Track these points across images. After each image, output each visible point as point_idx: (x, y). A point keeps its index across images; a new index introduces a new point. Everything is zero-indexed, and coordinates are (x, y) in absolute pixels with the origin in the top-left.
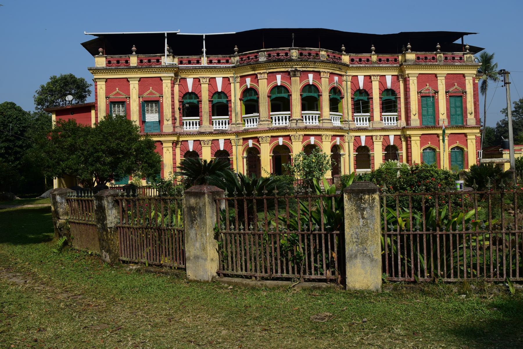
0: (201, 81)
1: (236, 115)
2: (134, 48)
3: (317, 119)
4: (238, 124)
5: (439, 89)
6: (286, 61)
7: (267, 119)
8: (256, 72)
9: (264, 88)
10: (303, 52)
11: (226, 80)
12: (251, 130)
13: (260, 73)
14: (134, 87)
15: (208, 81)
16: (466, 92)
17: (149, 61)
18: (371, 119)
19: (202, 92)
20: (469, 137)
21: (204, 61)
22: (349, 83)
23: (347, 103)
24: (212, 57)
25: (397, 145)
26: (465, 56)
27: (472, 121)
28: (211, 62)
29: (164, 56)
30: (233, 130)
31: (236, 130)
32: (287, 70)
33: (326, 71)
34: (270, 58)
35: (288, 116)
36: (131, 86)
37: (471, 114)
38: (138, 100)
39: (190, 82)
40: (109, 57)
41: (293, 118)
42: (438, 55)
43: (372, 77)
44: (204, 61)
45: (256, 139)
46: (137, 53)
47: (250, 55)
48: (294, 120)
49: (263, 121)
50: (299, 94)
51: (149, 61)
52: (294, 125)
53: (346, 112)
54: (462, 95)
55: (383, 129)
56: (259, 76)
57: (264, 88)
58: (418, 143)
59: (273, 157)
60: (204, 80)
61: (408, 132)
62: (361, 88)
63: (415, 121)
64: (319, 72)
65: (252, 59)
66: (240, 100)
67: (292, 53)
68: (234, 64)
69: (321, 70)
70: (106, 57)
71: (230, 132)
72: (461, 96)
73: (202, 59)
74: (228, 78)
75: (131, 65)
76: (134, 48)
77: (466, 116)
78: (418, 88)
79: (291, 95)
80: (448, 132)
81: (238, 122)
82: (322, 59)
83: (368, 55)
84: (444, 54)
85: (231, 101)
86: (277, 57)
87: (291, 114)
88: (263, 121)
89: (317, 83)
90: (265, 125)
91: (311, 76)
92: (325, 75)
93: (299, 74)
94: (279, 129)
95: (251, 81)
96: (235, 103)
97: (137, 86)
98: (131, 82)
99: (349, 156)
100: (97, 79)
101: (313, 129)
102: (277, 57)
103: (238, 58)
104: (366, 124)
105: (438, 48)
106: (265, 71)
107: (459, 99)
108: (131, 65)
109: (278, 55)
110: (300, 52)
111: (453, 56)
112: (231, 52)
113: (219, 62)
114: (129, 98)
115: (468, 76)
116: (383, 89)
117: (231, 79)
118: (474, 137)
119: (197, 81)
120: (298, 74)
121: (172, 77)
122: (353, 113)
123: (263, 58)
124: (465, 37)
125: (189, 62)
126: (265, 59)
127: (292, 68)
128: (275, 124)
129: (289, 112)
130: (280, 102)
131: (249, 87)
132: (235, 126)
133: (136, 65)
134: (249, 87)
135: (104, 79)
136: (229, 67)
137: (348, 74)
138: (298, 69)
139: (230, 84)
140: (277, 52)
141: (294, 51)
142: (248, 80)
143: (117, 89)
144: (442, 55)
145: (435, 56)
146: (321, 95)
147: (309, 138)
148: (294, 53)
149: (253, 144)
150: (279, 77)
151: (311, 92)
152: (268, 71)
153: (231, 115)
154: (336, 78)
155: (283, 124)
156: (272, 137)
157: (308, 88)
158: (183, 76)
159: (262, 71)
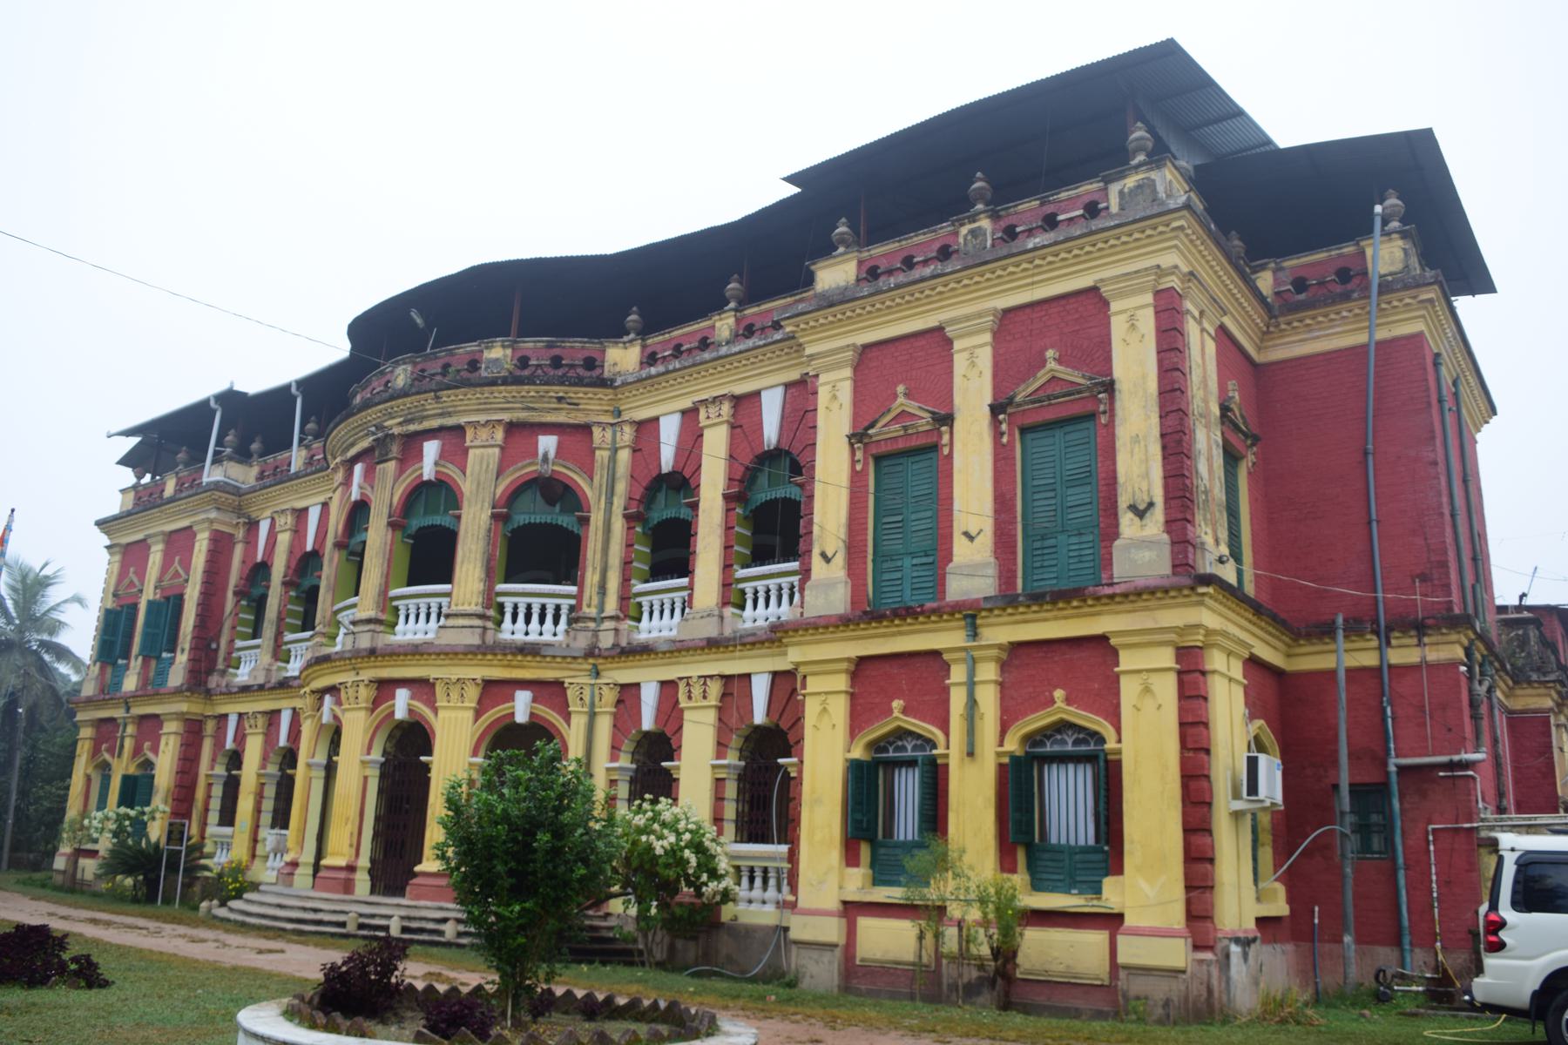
5: (957, 400)
16: (1110, 387)
20: (1127, 661)
22: (624, 456)
23: (608, 539)
25: (784, 725)
26: (1114, 189)
27: (1147, 555)
33: (482, 418)
37: (1140, 513)
53: (597, 578)
54: (1090, 407)
55: (714, 645)
58: (839, 708)
63: (829, 584)
64: (460, 430)
69: (462, 420)
72: (1085, 413)
80: (1002, 632)
82: (484, 374)
84: (995, 217)
89: (452, 471)
91: (431, 449)
92: (484, 434)
105: (980, 196)
107: (1076, 434)
111: (1049, 209)
115: (1122, 294)
118: (1166, 657)
120: (395, 449)
121: (211, 521)
122: (625, 581)
137: (626, 416)
138: (396, 431)
144: (985, 223)
145: (949, 241)
147: (393, 697)
151: (436, 511)
154: (547, 443)
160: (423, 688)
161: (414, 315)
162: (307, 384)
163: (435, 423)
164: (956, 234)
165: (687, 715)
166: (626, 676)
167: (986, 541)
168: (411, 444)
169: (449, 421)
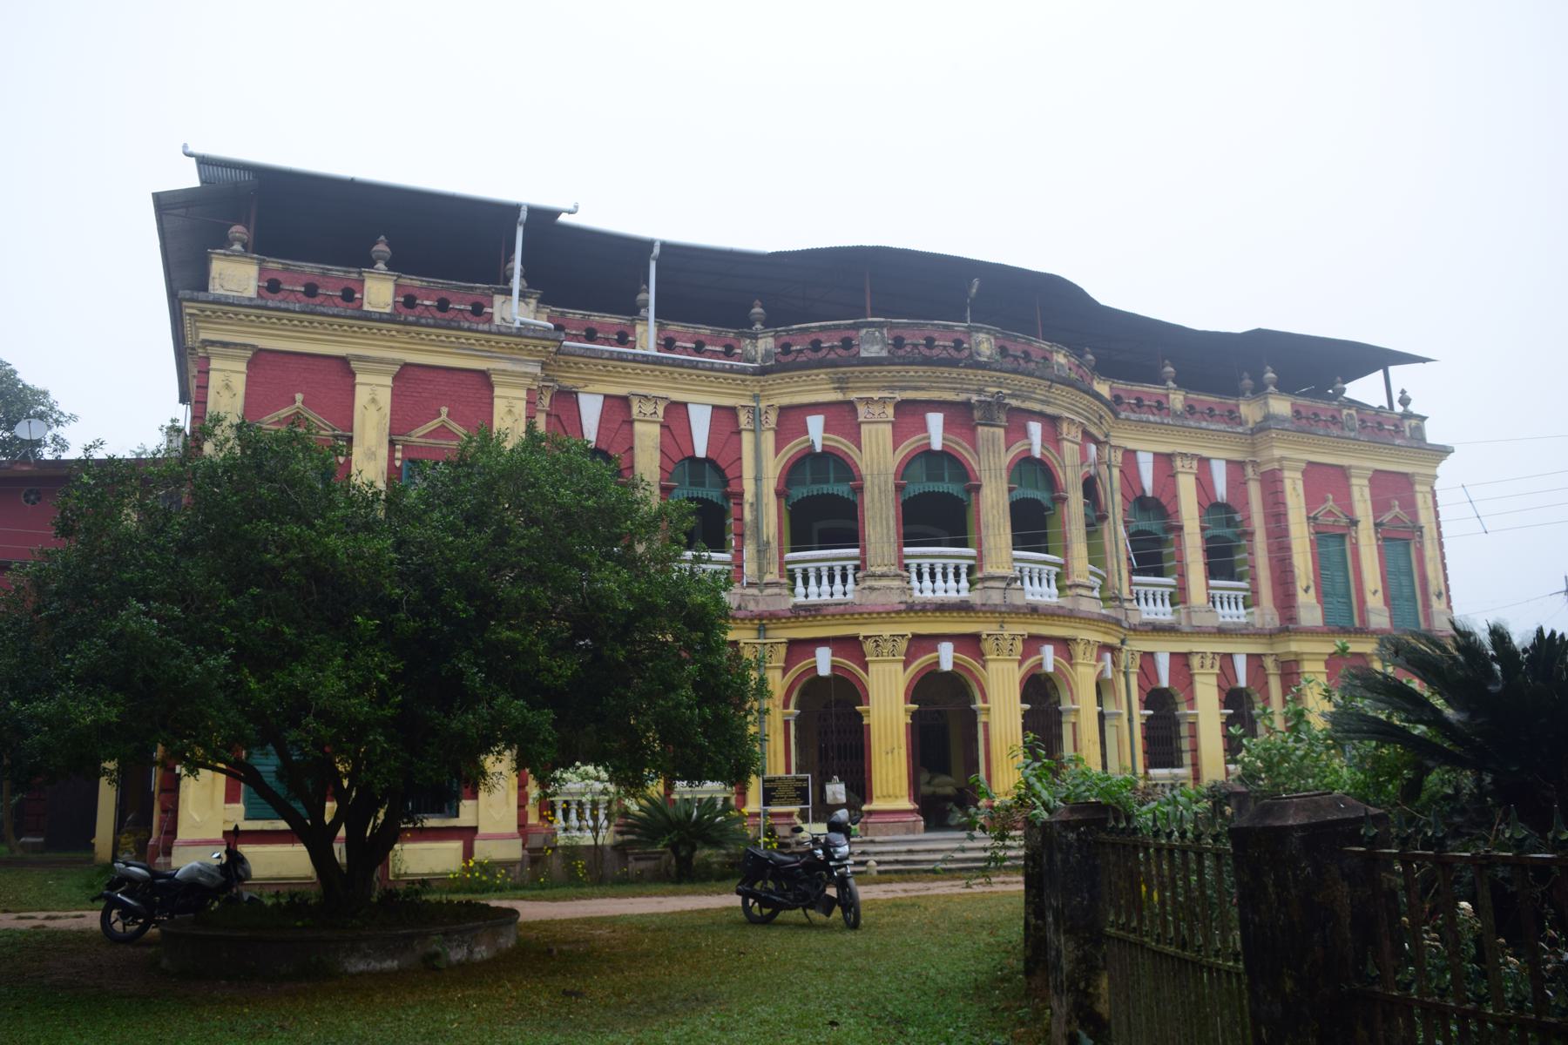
0: (635, 410)
1: (762, 550)
2: (381, 248)
3: (1053, 583)
4: (768, 585)
6: (966, 366)
7: (894, 569)
8: (853, 396)
9: (878, 455)
10: (1007, 344)
11: (724, 416)
12: (832, 609)
13: (869, 401)
14: (373, 402)
15: (661, 412)
16: (1420, 529)
17: (443, 305)
18: (1179, 597)
19: (637, 451)
21: (647, 337)
22: (1116, 472)
24: (674, 328)
28: (668, 344)
29: (509, 292)
30: (752, 606)
31: (762, 607)
32: (962, 397)
34: (901, 352)
35: (964, 564)
36: (362, 395)
38: (384, 452)
39: (591, 409)
40: (274, 265)
41: (989, 569)
42: (1345, 412)
43: (1178, 463)
44: (647, 337)
45: (849, 646)
46: (393, 265)
47: (823, 336)
48: (993, 578)
49: (883, 576)
50: (1005, 487)
51: (443, 305)
52: (996, 598)
55: (1222, 632)
56: (862, 410)
57: (878, 455)
59: (914, 715)
60: (648, 408)
61: (1295, 646)
62: (1149, 493)
63: (1309, 609)
65: (832, 348)
66: (779, 494)
67: (978, 344)
68: (754, 361)
70: (261, 263)
71: (741, 614)
73: (639, 329)
74: (732, 411)
75: (366, 307)
76: (381, 248)
77: (1427, 605)
78: (1307, 504)
79: (978, 488)
81: (768, 578)
83: (1157, 390)
85: (741, 495)
86: (927, 352)
87: (980, 557)
88: (883, 576)
90: (889, 594)
93: (1003, 418)
94: (942, 608)
95: (827, 429)
96: (757, 506)
97: (385, 397)
98: (359, 378)
99: (1130, 720)
100: (213, 343)
101: (1053, 615)
102: (927, 352)
103: (766, 343)
104: (1162, 613)
106: (886, 394)
108: (366, 307)
109: (930, 343)
110: (1002, 342)
112: (738, 319)
113: (699, 349)
114: (350, 440)
115: (1422, 483)
116: (1207, 505)
117: (743, 418)
119: (618, 407)
122: (1133, 572)
123: (876, 348)
124: (1392, 369)
125: (591, 336)
126: (884, 354)
127: (980, 392)
128: (927, 592)
129: (971, 551)
130: (937, 514)
131: (818, 449)
132: (755, 591)
133: (388, 310)
134: (818, 449)
135: (244, 346)
136: (731, 370)
137: (1114, 442)
139: (739, 432)
140: (927, 333)
141: (982, 336)
142: (815, 425)
143: (299, 397)
146: (1065, 499)
148: (985, 345)
149: (834, 667)
150: (935, 421)
152: (899, 396)
153: (740, 551)
155: (950, 591)
156: (917, 637)
157: (1030, 469)
158: (568, 383)
159: (876, 395)
160: (1064, 646)
161: (976, 282)
162: (673, 252)
163: (1037, 407)
164: (1340, 411)
165: (1197, 678)
166: (1147, 646)
167: (1380, 595)
168: (1017, 420)
169: (1049, 410)
